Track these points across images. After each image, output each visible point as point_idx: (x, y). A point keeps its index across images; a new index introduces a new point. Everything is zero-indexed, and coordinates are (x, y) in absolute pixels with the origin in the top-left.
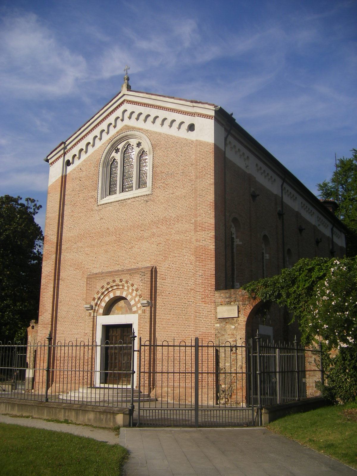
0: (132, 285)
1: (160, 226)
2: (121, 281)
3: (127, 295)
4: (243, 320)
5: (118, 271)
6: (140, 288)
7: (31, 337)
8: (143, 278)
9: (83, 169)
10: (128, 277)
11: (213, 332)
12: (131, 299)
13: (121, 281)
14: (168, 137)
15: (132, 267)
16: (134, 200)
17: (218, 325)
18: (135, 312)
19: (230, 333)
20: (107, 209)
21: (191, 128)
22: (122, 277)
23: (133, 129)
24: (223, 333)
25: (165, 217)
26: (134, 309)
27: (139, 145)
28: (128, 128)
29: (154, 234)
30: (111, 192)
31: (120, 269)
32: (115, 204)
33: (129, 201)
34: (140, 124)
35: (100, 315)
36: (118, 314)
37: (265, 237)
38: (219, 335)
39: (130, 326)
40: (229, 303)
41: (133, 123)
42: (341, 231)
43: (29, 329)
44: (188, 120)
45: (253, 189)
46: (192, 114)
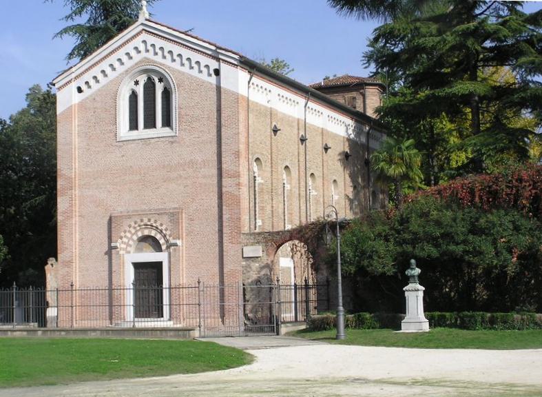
1: (186, 168)
2: (149, 220)
5: (145, 210)
7: (51, 275)
8: (172, 218)
9: (97, 98)
10: (157, 217)
11: (241, 269)
13: (149, 220)
14: (191, 77)
15: (160, 207)
16: (157, 140)
17: (244, 263)
20: (129, 146)
21: (217, 72)
22: (150, 216)
24: (248, 269)
26: (164, 247)
28: (147, 60)
29: (181, 176)
33: (153, 141)
34: (159, 59)
35: (129, 252)
36: (146, 252)
37: (287, 167)
38: (245, 272)
39: (161, 263)
40: (252, 244)
41: (150, 55)
42: (381, 132)
43: (48, 268)
44: (214, 64)
45: (274, 124)
46: (218, 60)
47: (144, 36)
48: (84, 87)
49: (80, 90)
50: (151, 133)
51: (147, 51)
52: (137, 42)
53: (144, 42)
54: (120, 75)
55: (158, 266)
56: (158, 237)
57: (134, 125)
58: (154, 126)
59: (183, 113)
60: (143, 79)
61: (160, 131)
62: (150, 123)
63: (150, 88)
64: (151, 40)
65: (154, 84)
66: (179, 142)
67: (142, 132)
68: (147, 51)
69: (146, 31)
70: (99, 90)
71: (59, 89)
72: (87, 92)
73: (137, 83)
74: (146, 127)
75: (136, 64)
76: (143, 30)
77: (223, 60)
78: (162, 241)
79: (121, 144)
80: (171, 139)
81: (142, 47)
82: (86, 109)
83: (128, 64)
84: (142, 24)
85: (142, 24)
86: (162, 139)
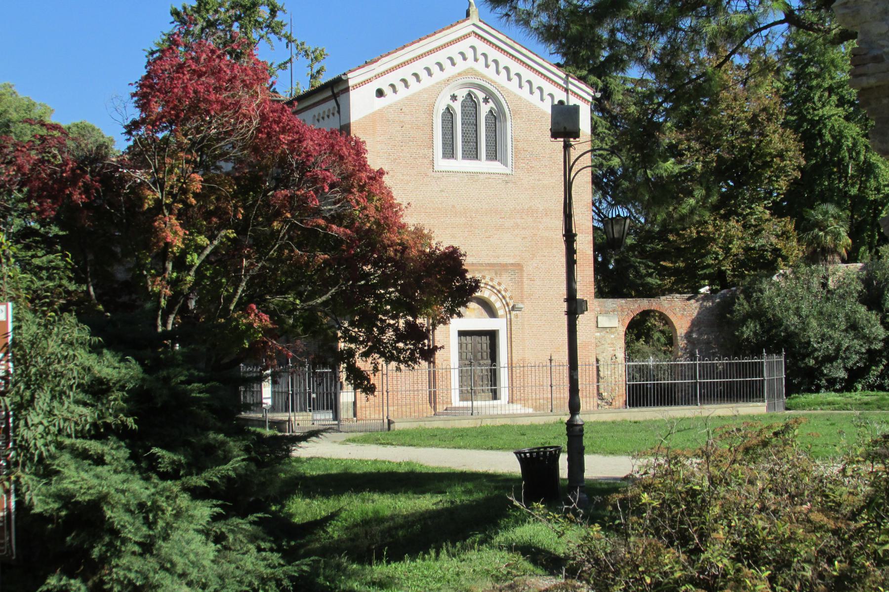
0: (499, 284)
3: (490, 296)
4: (622, 330)
6: (510, 289)
11: (593, 341)
12: (496, 301)
15: (492, 261)
16: (489, 176)
17: (598, 334)
18: (502, 316)
19: (609, 341)
23: (483, 77)
25: (530, 207)
26: (501, 312)
27: (486, 101)
29: (518, 226)
30: (449, 152)
31: (475, 261)
32: (461, 175)
33: (482, 177)
34: (491, 72)
41: (480, 66)
47: (474, 40)
48: (387, 90)
49: (380, 93)
50: (471, 165)
51: (476, 60)
52: (464, 46)
53: (473, 48)
54: (437, 84)
55: (492, 335)
56: (493, 299)
57: (449, 152)
58: (476, 157)
59: (520, 145)
60: (462, 94)
61: (482, 165)
62: (472, 153)
63: (471, 104)
64: (482, 47)
65: (475, 106)
66: (515, 183)
67: (460, 164)
68: (476, 60)
69: (476, 34)
70: (407, 98)
71: (356, 86)
72: (390, 97)
73: (454, 98)
74: (464, 158)
75: (459, 74)
76: (474, 32)
77: (573, 92)
78: (498, 305)
79: (440, 175)
80: (504, 177)
81: (470, 54)
82: (388, 121)
83: (450, 71)
84: (474, 25)
85: (474, 25)
86: (494, 176)
